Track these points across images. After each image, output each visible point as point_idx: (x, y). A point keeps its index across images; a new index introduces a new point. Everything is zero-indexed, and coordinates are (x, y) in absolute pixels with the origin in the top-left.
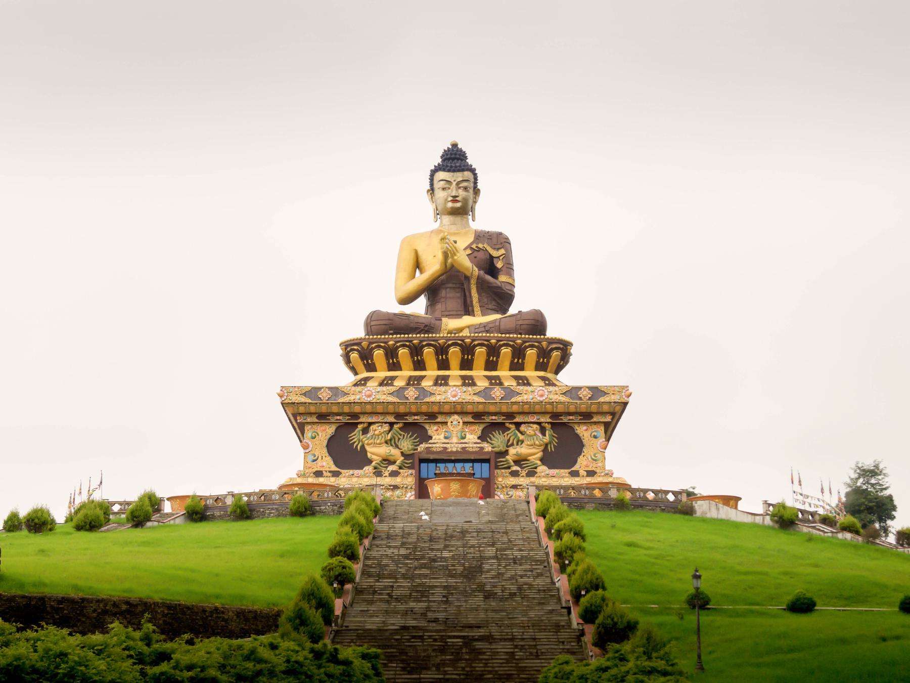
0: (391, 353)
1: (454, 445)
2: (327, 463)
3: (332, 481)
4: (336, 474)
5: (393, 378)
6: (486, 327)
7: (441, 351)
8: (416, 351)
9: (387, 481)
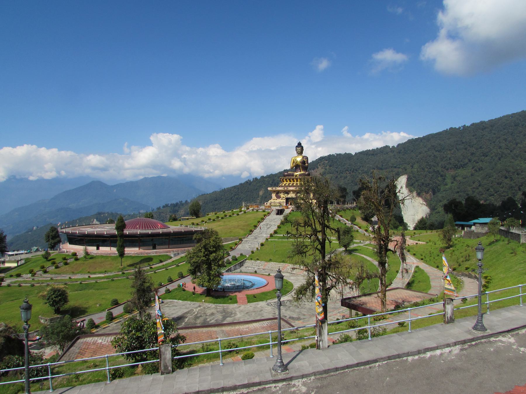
0: (286, 180)
1: (290, 197)
2: (275, 198)
3: (276, 201)
4: (276, 200)
5: (286, 183)
6: (300, 175)
7: (293, 179)
8: (289, 180)
9: (283, 201)
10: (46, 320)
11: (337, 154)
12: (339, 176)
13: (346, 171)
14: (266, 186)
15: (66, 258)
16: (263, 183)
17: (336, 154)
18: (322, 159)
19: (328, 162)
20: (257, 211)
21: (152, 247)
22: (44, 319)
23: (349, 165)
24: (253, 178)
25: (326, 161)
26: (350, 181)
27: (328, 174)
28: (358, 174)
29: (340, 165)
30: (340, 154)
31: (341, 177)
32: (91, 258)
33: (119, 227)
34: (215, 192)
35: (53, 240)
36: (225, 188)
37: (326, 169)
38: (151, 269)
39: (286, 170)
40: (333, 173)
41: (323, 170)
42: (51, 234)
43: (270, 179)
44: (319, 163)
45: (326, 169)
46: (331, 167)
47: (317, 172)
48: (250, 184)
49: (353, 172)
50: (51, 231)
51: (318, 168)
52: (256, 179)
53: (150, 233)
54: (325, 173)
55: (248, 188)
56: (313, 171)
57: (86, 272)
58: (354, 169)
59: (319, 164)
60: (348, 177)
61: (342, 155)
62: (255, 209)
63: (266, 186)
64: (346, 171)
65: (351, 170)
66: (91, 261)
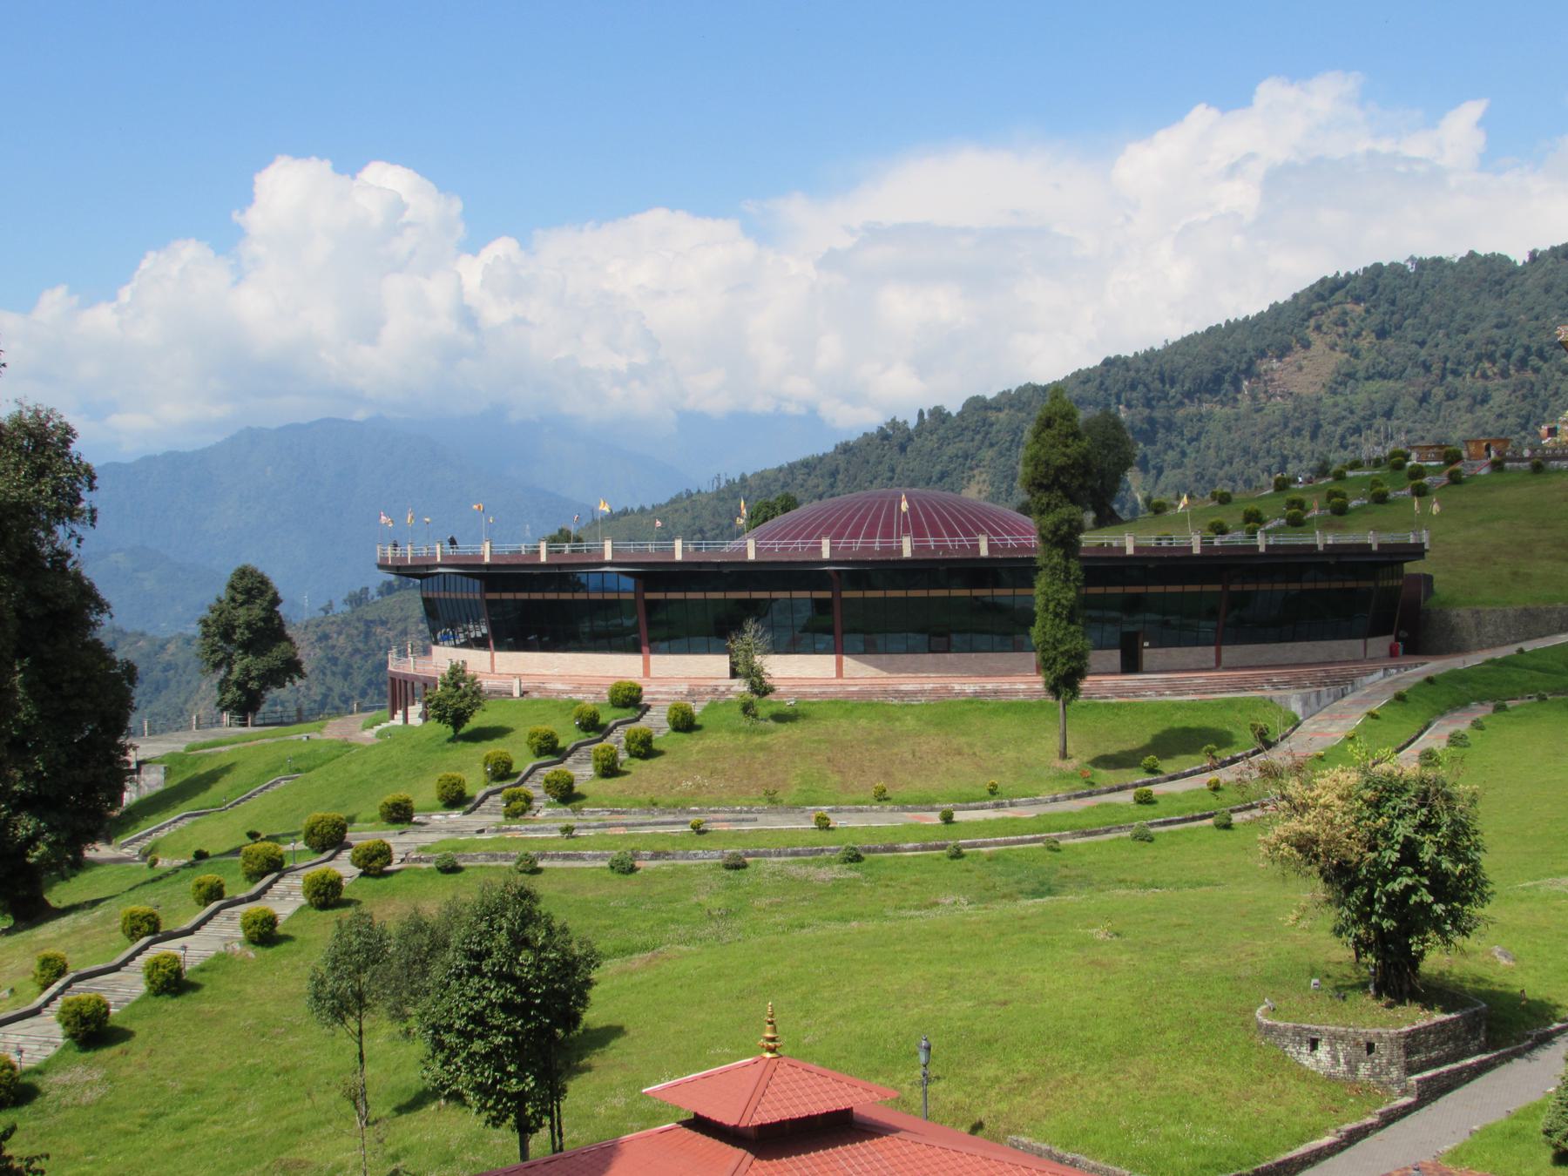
10: (1370, 1048)
11: (1421, 264)
12: (1439, 393)
13: (1479, 358)
14: (1001, 454)
15: (602, 720)
16: (978, 437)
17: (1412, 259)
18: (1328, 290)
19: (1367, 311)
20: (1538, 468)
21: (1117, 653)
22: (1334, 1038)
23: (1498, 327)
24: (921, 414)
25: (1358, 300)
26: (1512, 420)
27: (1368, 378)
28: (1558, 375)
29: (1439, 327)
30: (1438, 261)
31: (1449, 398)
32: (780, 718)
33: (1061, 470)
34: (690, 495)
35: (259, 653)
36: (749, 474)
37: (1355, 354)
38: (1148, 810)
39: (1118, 358)
40: (1399, 375)
41: (1340, 357)
42: (242, 614)
43: (1022, 415)
44: (1311, 314)
45: (1355, 354)
46: (1389, 341)
47: (1300, 368)
48: (903, 448)
49: (1523, 363)
50: (240, 598)
51: (1307, 345)
52: (939, 414)
53: (1130, 551)
54: (1350, 376)
55: (893, 470)
56: (1275, 364)
57: (862, 797)
58: (1527, 349)
59: (1312, 322)
60: (1498, 399)
61: (1452, 266)
62: (1522, 460)
63: (1001, 454)
64: (1479, 358)
65: (1507, 355)
66: (785, 729)
